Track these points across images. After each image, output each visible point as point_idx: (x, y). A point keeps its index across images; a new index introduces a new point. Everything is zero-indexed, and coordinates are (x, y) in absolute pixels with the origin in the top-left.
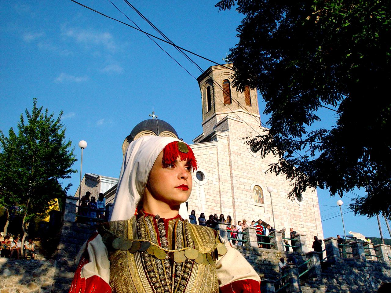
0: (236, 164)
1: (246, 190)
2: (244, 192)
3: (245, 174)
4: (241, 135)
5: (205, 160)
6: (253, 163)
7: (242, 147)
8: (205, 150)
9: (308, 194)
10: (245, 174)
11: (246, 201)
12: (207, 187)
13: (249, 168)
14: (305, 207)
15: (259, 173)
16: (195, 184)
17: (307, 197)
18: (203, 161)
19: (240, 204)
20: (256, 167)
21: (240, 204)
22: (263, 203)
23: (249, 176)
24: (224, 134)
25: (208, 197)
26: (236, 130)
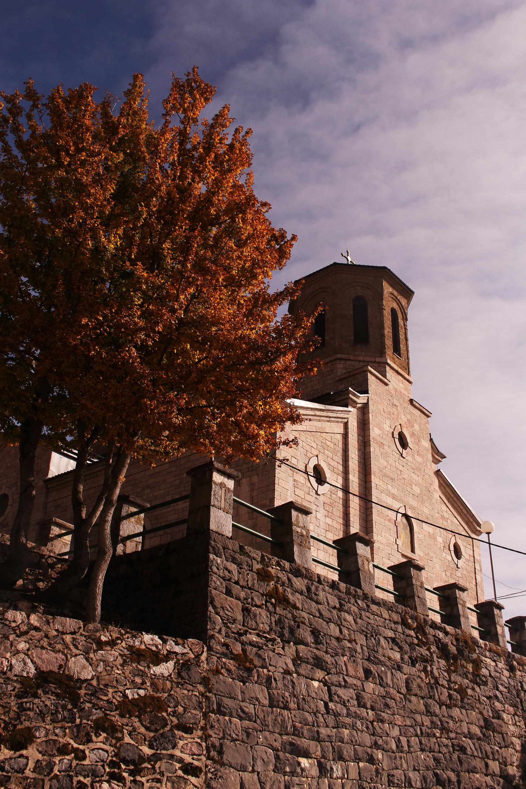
0: (376, 463)
1: (390, 520)
2: (387, 523)
3: (390, 487)
4: (385, 409)
5: (328, 443)
6: (401, 468)
7: (386, 433)
8: (329, 423)
9: (468, 546)
10: (390, 487)
11: (389, 542)
12: (328, 501)
13: (396, 477)
14: (465, 572)
15: (409, 489)
16: (311, 490)
17: (468, 552)
18: (325, 445)
19: (381, 546)
20: (405, 476)
21: (381, 546)
22: (413, 551)
23: (395, 491)
24: (362, 399)
25: (329, 521)
26: (378, 397)
